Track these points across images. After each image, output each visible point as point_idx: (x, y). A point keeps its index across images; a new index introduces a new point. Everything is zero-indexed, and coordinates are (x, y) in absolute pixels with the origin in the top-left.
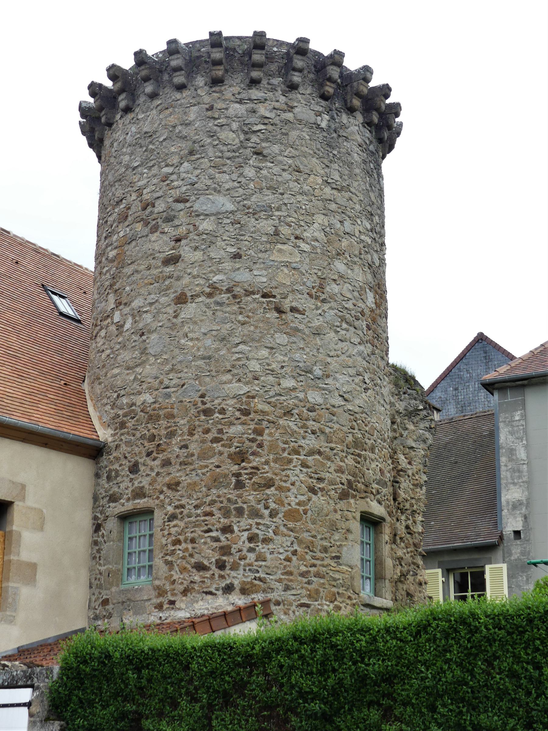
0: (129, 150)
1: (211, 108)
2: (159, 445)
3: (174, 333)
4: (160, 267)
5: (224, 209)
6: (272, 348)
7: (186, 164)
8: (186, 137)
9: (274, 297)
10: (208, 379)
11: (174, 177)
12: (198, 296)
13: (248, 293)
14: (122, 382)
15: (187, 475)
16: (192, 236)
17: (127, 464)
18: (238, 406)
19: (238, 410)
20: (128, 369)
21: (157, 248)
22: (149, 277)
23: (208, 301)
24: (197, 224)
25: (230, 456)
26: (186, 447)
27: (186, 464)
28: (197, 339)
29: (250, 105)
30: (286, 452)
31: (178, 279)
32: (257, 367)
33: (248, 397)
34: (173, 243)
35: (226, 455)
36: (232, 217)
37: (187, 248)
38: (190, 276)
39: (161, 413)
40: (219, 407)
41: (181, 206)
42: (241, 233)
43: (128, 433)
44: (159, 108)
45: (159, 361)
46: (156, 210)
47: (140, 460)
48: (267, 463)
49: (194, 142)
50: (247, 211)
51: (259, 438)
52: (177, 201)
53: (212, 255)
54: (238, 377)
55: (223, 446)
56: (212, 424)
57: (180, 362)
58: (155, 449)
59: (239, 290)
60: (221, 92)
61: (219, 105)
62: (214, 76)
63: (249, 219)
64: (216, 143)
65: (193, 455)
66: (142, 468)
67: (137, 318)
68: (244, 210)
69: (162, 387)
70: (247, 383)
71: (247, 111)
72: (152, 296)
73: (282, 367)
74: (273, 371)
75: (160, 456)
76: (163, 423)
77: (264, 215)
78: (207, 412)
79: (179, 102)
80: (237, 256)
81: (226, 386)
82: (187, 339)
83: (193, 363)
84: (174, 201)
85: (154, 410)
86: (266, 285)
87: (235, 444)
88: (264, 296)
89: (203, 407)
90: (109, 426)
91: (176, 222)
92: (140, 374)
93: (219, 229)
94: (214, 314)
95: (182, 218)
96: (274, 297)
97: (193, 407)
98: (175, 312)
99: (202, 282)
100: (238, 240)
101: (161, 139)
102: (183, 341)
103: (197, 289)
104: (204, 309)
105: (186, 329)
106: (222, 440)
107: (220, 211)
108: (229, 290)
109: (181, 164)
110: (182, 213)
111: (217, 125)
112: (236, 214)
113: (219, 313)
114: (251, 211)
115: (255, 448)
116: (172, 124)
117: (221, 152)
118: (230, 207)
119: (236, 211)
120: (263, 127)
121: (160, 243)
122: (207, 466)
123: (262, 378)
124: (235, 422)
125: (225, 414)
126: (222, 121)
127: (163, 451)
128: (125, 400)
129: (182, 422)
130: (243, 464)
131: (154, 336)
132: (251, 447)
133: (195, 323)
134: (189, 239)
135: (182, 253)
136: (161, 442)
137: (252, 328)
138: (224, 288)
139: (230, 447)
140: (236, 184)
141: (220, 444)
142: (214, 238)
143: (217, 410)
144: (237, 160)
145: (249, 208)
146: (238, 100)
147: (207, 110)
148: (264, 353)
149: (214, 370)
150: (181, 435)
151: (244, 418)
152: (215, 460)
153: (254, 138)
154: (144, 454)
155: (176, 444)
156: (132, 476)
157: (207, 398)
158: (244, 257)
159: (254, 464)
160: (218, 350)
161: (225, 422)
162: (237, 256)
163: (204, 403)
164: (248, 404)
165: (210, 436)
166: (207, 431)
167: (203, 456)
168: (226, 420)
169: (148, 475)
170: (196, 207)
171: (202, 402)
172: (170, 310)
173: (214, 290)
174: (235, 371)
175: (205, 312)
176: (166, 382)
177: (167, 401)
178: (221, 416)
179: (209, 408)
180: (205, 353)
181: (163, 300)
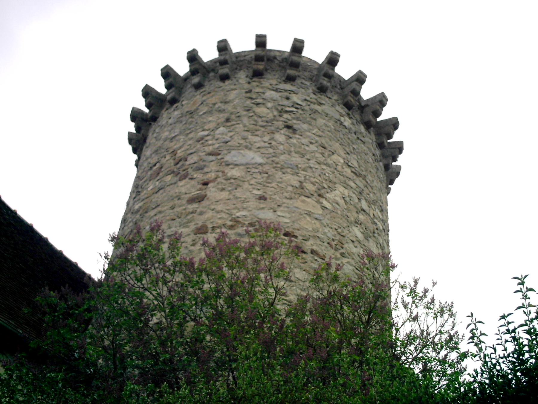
5: (253, 161)
9: (296, 237)
24: (226, 171)
31: (201, 213)
37: (213, 190)
49: (232, 113)
52: (210, 154)
53: (238, 195)
60: (260, 82)
63: (276, 172)
80: (262, 198)
84: (206, 155)
86: (289, 225)
91: (206, 170)
95: (213, 167)
101: (201, 113)
110: (212, 163)
112: (264, 166)
114: (279, 165)
119: (265, 164)
126: (259, 101)
138: (247, 223)
140: (266, 144)
146: (275, 89)
147: (246, 92)
158: (268, 200)
162: (262, 198)
170: (228, 158)
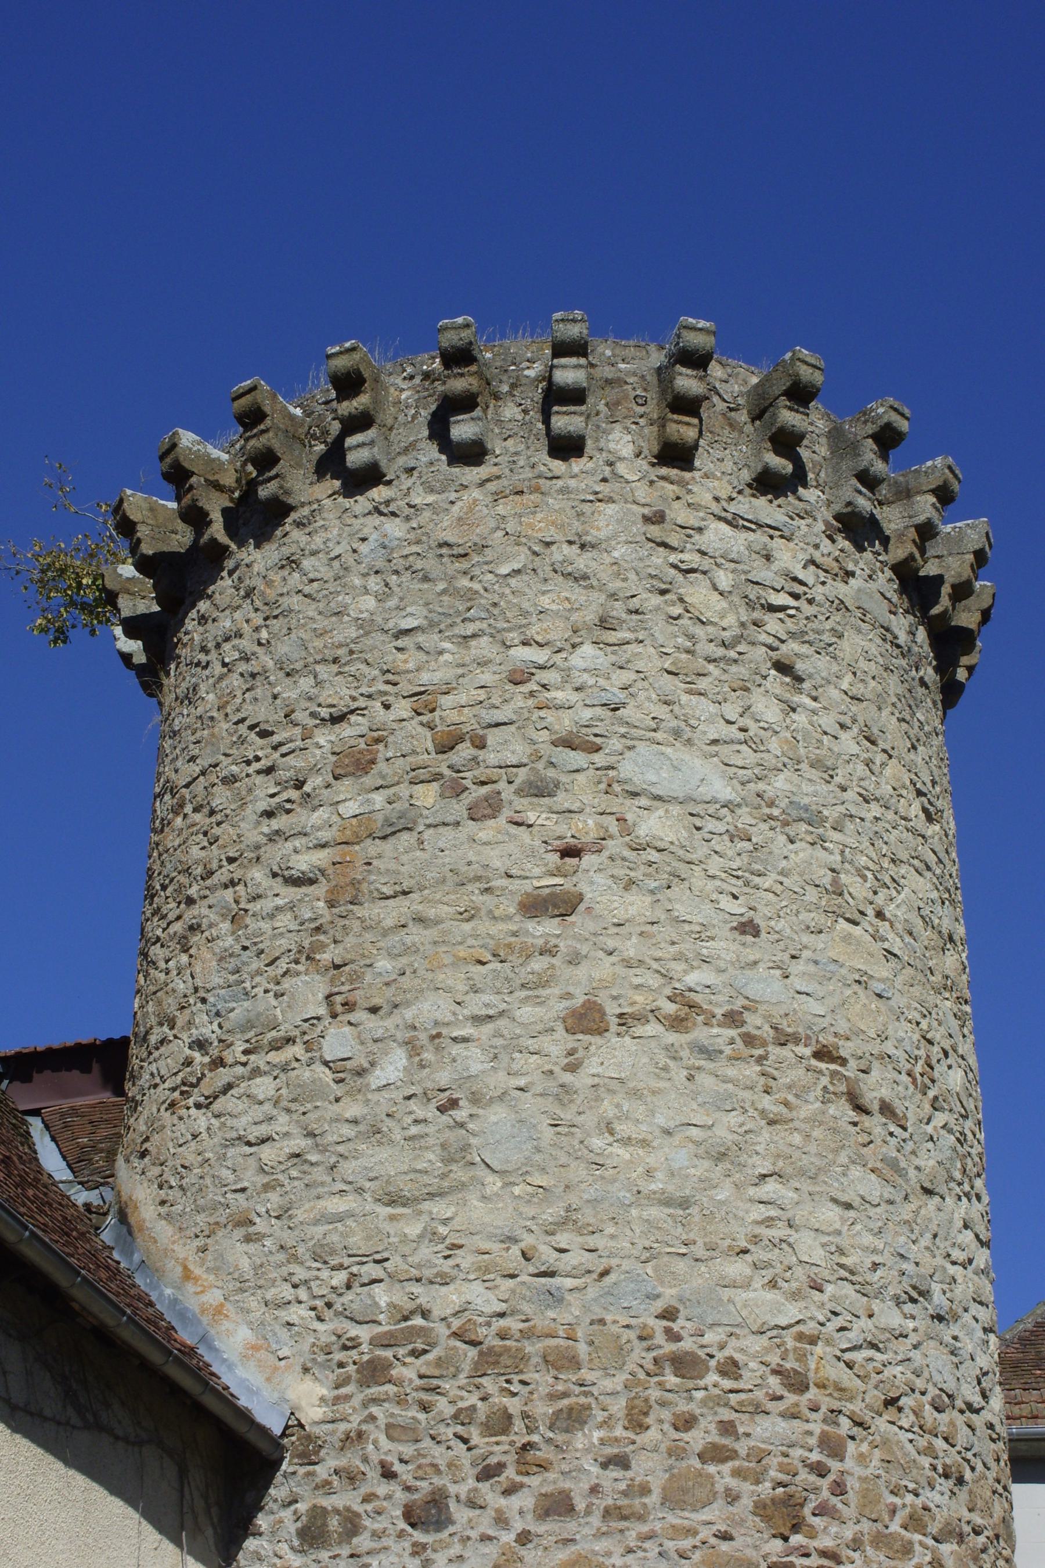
0: (374, 583)
1: (657, 518)
2: (526, 1447)
3: (567, 1115)
4: (509, 918)
5: (705, 792)
6: (848, 1206)
7: (588, 649)
8: (585, 577)
9: (843, 1062)
10: (681, 1266)
11: (550, 677)
12: (640, 1018)
13: (784, 1040)
14: (368, 1238)
15: (630, 1551)
16: (614, 846)
17: (394, 1497)
18: (774, 1359)
19: (775, 1372)
20: (391, 1203)
21: (497, 863)
22: (471, 942)
23: (671, 1037)
24: (629, 817)
25: (761, 1508)
26: (622, 1462)
27: (625, 1518)
28: (644, 1143)
29: (759, 538)
30: (898, 1519)
31: (575, 960)
32: (818, 1255)
33: (800, 1337)
34: (555, 857)
35: (747, 1502)
36: (729, 819)
37: (600, 879)
38: (613, 959)
39: (530, 1348)
40: (720, 1356)
41: (578, 759)
42: (756, 867)
43: (401, 1401)
44: (491, 486)
45: (517, 1190)
46: (491, 757)
47: (453, 1489)
48: (856, 1544)
49: (613, 596)
50: (767, 811)
51: (834, 1465)
52: (568, 743)
53: (681, 910)
54: (768, 1274)
55: (737, 1473)
56: (704, 1402)
57: (594, 1202)
58: (510, 1459)
59: (759, 1022)
60: (682, 483)
61: (679, 514)
62: (675, 438)
63: (771, 834)
64: (677, 610)
65: (645, 1490)
66: (461, 1514)
67: (428, 1056)
68: (759, 807)
69: (532, 1270)
70: (795, 1296)
71: (749, 548)
72: (486, 998)
73: (875, 1266)
74: (852, 1273)
75: (534, 1481)
76: (543, 1380)
77: (808, 832)
78: (686, 1365)
79: (560, 483)
80: (748, 928)
81: (741, 1296)
82: (611, 1139)
83: (634, 1212)
84: (554, 744)
85: (503, 1336)
86: (824, 1023)
87: (772, 1473)
88: (818, 1055)
89: (670, 1348)
90: (306, 1370)
91: (562, 801)
92: (445, 1222)
93: (696, 844)
94: (690, 1078)
95: (581, 791)
96: (843, 1062)
97: (638, 1346)
98: (570, 1053)
99: (654, 981)
100: (747, 884)
101: (504, 570)
102: (597, 1142)
103: (639, 998)
104: (663, 1059)
105: (608, 1108)
106: (733, 1455)
107: (695, 795)
108: (733, 1019)
109: (574, 646)
110: (581, 778)
111: (674, 566)
112: (739, 811)
113: (705, 1080)
114: (776, 812)
115: (825, 1494)
116: (540, 535)
117: (691, 637)
118: (726, 792)
119: (739, 805)
120: (791, 602)
121: (512, 851)
122: (691, 1532)
123: (829, 1289)
124: (770, 1406)
125: (738, 1378)
126: (691, 558)
127: (543, 1466)
128: (382, 1296)
129: (608, 1384)
130: (796, 1539)
131: (497, 1115)
132: (816, 1490)
133: (635, 1094)
134: (606, 853)
135: (584, 888)
136: (535, 1438)
137: (797, 1139)
138: (719, 1011)
139: (757, 1482)
140: (733, 732)
141: (727, 1468)
142: (682, 866)
143: (713, 1363)
144: (734, 669)
145: (771, 804)
146: (729, 516)
147: (647, 519)
148: (830, 1215)
149: (700, 1242)
150: (605, 1424)
151: (791, 1398)
152: (715, 1513)
153: (773, 624)
154: (470, 1472)
155: (587, 1451)
156: (419, 1536)
157: (681, 1322)
158: (763, 935)
159: (826, 1542)
160: (706, 1184)
161: (741, 1403)
162: (748, 928)
163: (673, 1337)
164: (802, 1357)
165: (696, 1439)
166: (686, 1423)
167: (676, 1497)
168: (743, 1396)
169: (485, 1538)
170: (627, 769)
171: (668, 1331)
172: (556, 1045)
173: (686, 1011)
174: (759, 1254)
175: (666, 1069)
176: (547, 1256)
177: (551, 1314)
178: (727, 1384)
179: (693, 1354)
180: (671, 1188)
181: (526, 1013)
